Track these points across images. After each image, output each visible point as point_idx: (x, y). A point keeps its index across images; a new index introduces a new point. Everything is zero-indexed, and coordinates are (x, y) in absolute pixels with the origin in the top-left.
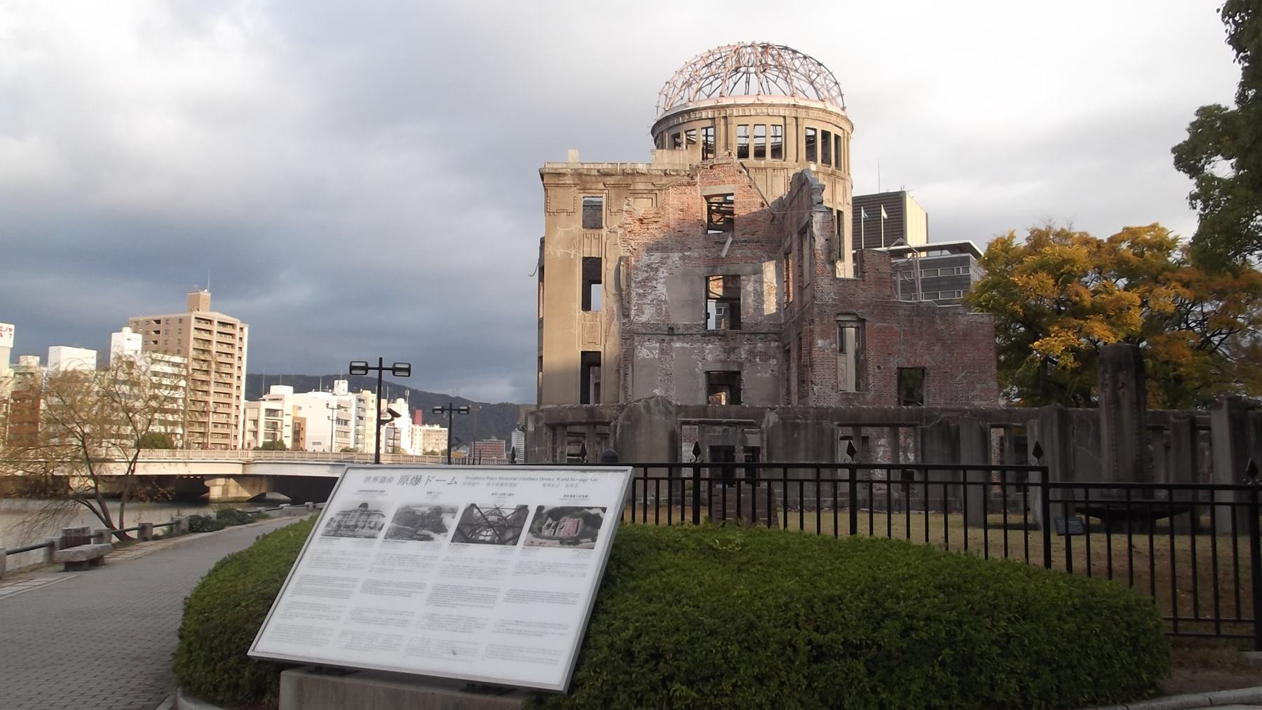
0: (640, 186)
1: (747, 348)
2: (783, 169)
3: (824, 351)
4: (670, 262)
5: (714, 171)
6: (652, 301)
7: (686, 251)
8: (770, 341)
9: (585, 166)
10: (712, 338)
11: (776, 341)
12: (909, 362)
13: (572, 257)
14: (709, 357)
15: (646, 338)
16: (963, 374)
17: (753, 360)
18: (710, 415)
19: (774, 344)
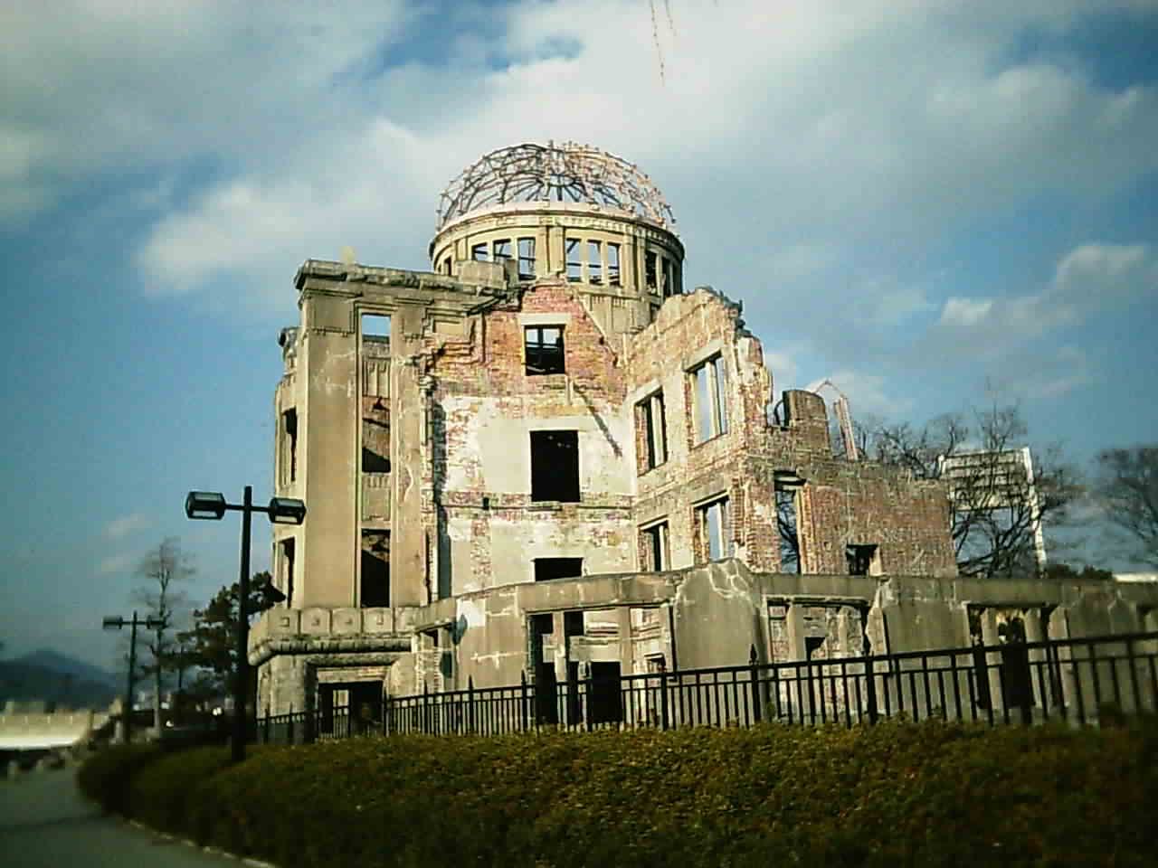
0: (443, 305)
1: (591, 526)
2: (624, 298)
3: (763, 520)
4: (481, 408)
5: (538, 293)
6: (461, 461)
7: (504, 396)
8: (619, 518)
9: (367, 272)
10: (543, 513)
11: (626, 518)
12: (860, 539)
13: (349, 395)
14: (540, 539)
15: (453, 511)
16: (921, 554)
17: (598, 544)
18: (806, 591)
19: (624, 522)
